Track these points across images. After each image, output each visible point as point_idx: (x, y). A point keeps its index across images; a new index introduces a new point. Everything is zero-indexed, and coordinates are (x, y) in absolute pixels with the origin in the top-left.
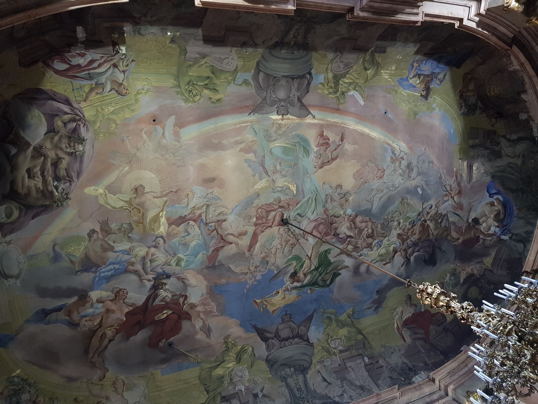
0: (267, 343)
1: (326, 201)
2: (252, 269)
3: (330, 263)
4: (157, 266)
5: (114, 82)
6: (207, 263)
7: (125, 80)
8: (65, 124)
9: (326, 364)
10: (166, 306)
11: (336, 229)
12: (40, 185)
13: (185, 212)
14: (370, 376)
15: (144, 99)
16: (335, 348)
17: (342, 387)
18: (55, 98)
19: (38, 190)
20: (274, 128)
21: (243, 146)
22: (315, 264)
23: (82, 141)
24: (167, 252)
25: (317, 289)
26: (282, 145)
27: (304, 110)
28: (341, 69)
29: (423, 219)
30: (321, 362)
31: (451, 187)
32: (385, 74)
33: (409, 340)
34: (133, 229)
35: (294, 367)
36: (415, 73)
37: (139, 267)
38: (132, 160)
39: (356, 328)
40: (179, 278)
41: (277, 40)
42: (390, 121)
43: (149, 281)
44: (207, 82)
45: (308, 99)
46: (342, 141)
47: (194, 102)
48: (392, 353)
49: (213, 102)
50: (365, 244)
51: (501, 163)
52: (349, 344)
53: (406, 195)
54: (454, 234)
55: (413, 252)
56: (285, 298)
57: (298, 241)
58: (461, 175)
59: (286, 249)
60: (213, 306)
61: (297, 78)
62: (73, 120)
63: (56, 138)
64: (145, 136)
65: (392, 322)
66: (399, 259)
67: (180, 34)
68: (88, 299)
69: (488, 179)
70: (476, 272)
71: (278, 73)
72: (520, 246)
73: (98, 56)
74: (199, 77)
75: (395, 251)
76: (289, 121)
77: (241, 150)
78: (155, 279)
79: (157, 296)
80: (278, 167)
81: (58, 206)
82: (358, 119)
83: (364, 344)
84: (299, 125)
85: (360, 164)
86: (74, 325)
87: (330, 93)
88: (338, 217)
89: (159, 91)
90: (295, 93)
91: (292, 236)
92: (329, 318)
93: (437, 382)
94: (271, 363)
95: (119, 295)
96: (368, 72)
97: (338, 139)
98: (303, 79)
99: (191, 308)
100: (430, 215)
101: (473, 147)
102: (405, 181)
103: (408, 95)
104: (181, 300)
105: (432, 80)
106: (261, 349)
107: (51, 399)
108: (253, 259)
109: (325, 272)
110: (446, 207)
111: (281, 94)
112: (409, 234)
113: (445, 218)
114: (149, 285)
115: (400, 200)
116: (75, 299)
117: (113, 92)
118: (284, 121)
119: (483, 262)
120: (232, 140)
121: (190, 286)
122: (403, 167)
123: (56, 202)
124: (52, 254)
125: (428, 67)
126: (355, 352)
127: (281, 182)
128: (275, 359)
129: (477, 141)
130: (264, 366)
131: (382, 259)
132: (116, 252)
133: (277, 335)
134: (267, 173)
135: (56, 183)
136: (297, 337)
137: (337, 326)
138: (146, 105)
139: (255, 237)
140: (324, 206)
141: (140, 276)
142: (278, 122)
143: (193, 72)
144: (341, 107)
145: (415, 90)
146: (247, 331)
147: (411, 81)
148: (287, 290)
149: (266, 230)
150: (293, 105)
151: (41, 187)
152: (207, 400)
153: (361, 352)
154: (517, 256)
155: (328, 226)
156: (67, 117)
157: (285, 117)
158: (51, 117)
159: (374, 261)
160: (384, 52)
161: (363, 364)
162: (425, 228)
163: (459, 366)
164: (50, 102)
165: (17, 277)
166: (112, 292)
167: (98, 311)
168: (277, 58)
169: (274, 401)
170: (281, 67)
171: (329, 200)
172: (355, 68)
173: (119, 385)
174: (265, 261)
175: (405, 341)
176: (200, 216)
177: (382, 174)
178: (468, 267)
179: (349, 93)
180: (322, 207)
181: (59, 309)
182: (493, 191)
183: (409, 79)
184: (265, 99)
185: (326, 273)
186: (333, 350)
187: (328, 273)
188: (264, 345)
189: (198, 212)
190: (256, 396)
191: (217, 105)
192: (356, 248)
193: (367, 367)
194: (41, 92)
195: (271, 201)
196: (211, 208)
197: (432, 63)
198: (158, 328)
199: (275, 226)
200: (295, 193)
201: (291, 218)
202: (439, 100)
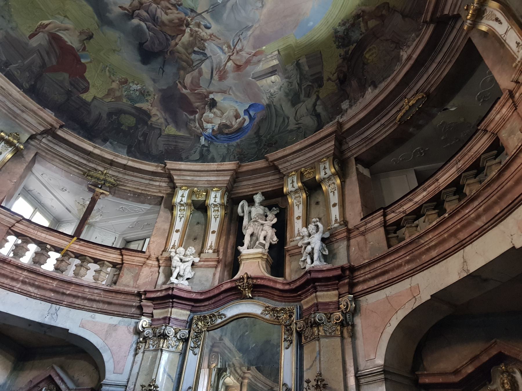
29: (189, 19)
31: (241, 50)
51: (288, 110)
55: (144, 20)
58: (259, 61)
69: (265, 101)
70: (154, 119)
72: (197, 156)
100: (197, 29)
101: (298, 65)
110: (216, 53)
119: (168, 125)
129: (307, 68)
154: (184, 156)
163: (18, 101)
178: (158, 110)
182: (252, 113)
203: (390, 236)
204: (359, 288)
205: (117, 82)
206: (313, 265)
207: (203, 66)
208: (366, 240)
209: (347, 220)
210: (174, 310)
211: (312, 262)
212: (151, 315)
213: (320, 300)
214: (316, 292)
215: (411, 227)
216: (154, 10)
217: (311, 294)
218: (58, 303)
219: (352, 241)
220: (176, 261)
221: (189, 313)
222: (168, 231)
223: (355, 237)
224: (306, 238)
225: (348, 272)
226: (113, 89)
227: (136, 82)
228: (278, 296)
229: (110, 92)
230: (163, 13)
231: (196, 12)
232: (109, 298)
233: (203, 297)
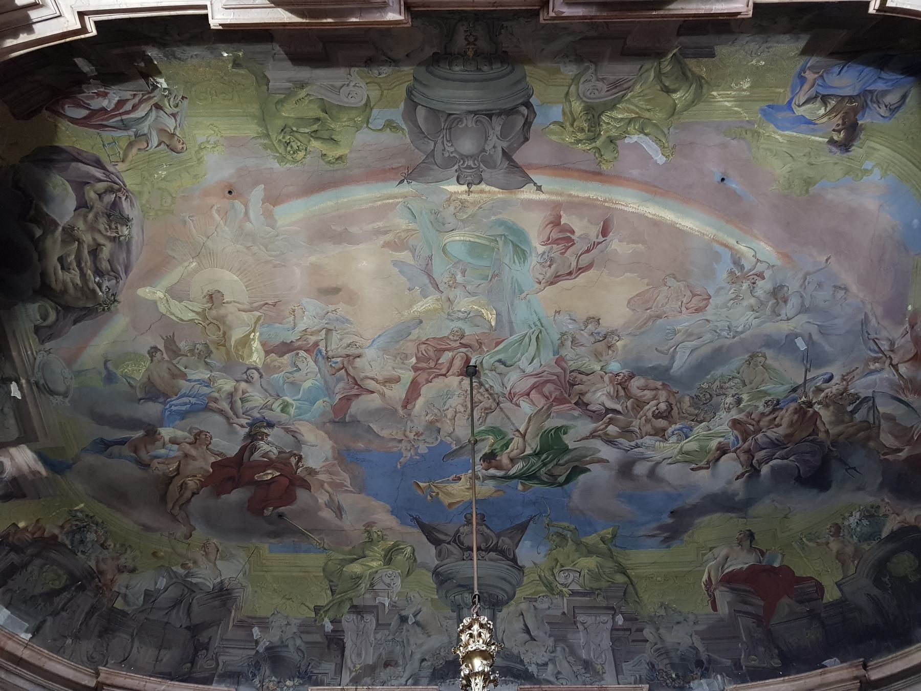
0: (439, 547)
1: (562, 344)
2: (411, 436)
3: (566, 450)
4: (252, 409)
5: (162, 131)
6: (332, 416)
7: (178, 129)
8: (100, 195)
9: (539, 605)
10: (270, 464)
11: (582, 394)
12: (78, 281)
13: (292, 337)
14: (613, 650)
15: (212, 158)
17: (552, 652)
18: (80, 158)
19: (75, 286)
20: (452, 208)
21: (389, 237)
23: (126, 221)
24: (266, 390)
25: (536, 487)
26: (468, 239)
27: (517, 174)
28: (603, 93)
29: (803, 399)
30: (530, 600)
31: (892, 344)
33: (724, 609)
34: (211, 352)
36: (812, 92)
37: (225, 406)
38: (200, 252)
39: (617, 562)
40: (287, 430)
41: (435, 50)
42: (734, 197)
43: (242, 426)
44: (315, 127)
45: (524, 155)
47: (295, 161)
48: (678, 623)
49: (329, 162)
50: (648, 428)
52: (595, 585)
53: (764, 350)
54: (887, 439)
57: (498, 404)
60: (345, 478)
61: (499, 114)
62: (110, 190)
63: (91, 216)
64: (216, 216)
65: (702, 568)
66: (730, 466)
67: (244, 54)
68: (158, 437)
71: (454, 107)
73: (128, 95)
74: (302, 119)
75: (723, 450)
76: (484, 195)
77: (386, 245)
78: (251, 425)
79: (254, 449)
80: (459, 277)
81: (104, 310)
83: (625, 593)
84: (505, 203)
85: (646, 281)
86: (144, 465)
87: (579, 141)
88: (588, 375)
89: (234, 144)
90: (495, 144)
91: (487, 395)
92: (563, 537)
94: (441, 578)
95: (199, 438)
96: (674, 96)
97: (594, 232)
99: (310, 474)
100: (823, 395)
102: (764, 322)
103: (791, 141)
104: (293, 461)
105: (864, 107)
106: (428, 554)
107: (122, 545)
108: (412, 421)
109: (555, 462)
110: (874, 382)
111: (467, 145)
112: (761, 423)
113: (865, 406)
114: (243, 432)
115: (746, 357)
116: (140, 434)
117: (162, 146)
120: (370, 227)
121: (305, 443)
122: (759, 292)
123: (101, 305)
124: (104, 373)
125: (847, 80)
126: (601, 601)
127: (464, 304)
130: (429, 579)
131: (687, 458)
132: (189, 381)
133: (457, 539)
134: (436, 286)
135: (97, 279)
137: (576, 550)
138: (217, 167)
139: (414, 390)
140: (556, 352)
141: (228, 418)
142: (460, 197)
143: (289, 112)
144: (604, 167)
146: (403, 523)
149: (436, 380)
151: (79, 282)
152: (330, 602)
153: (614, 604)
155: (566, 388)
156: (101, 186)
157: (474, 188)
158: (80, 185)
159: (669, 461)
160: (712, 55)
161: (609, 625)
162: (805, 415)
164: (74, 164)
165: (65, 395)
166: (190, 432)
167: (173, 454)
168: (448, 79)
169: (429, 636)
170: (459, 93)
172: (638, 88)
173: (212, 550)
174: (433, 427)
175: (715, 608)
176: (316, 344)
177: (702, 304)
179: (627, 141)
180: (551, 353)
181: (122, 442)
183: (793, 106)
184: (432, 154)
188: (432, 550)
189: (313, 339)
190: (404, 619)
191: (336, 166)
193: (614, 632)
194: (59, 150)
195: (446, 333)
196: (335, 336)
198: (259, 490)
199: (453, 375)
200: (493, 324)
201: (485, 365)
202: (883, 152)
205: (832, 539)
207: (881, 409)
216: (765, 439)
226: (837, 552)
229: (840, 556)
230: (775, 430)
231: (798, 387)
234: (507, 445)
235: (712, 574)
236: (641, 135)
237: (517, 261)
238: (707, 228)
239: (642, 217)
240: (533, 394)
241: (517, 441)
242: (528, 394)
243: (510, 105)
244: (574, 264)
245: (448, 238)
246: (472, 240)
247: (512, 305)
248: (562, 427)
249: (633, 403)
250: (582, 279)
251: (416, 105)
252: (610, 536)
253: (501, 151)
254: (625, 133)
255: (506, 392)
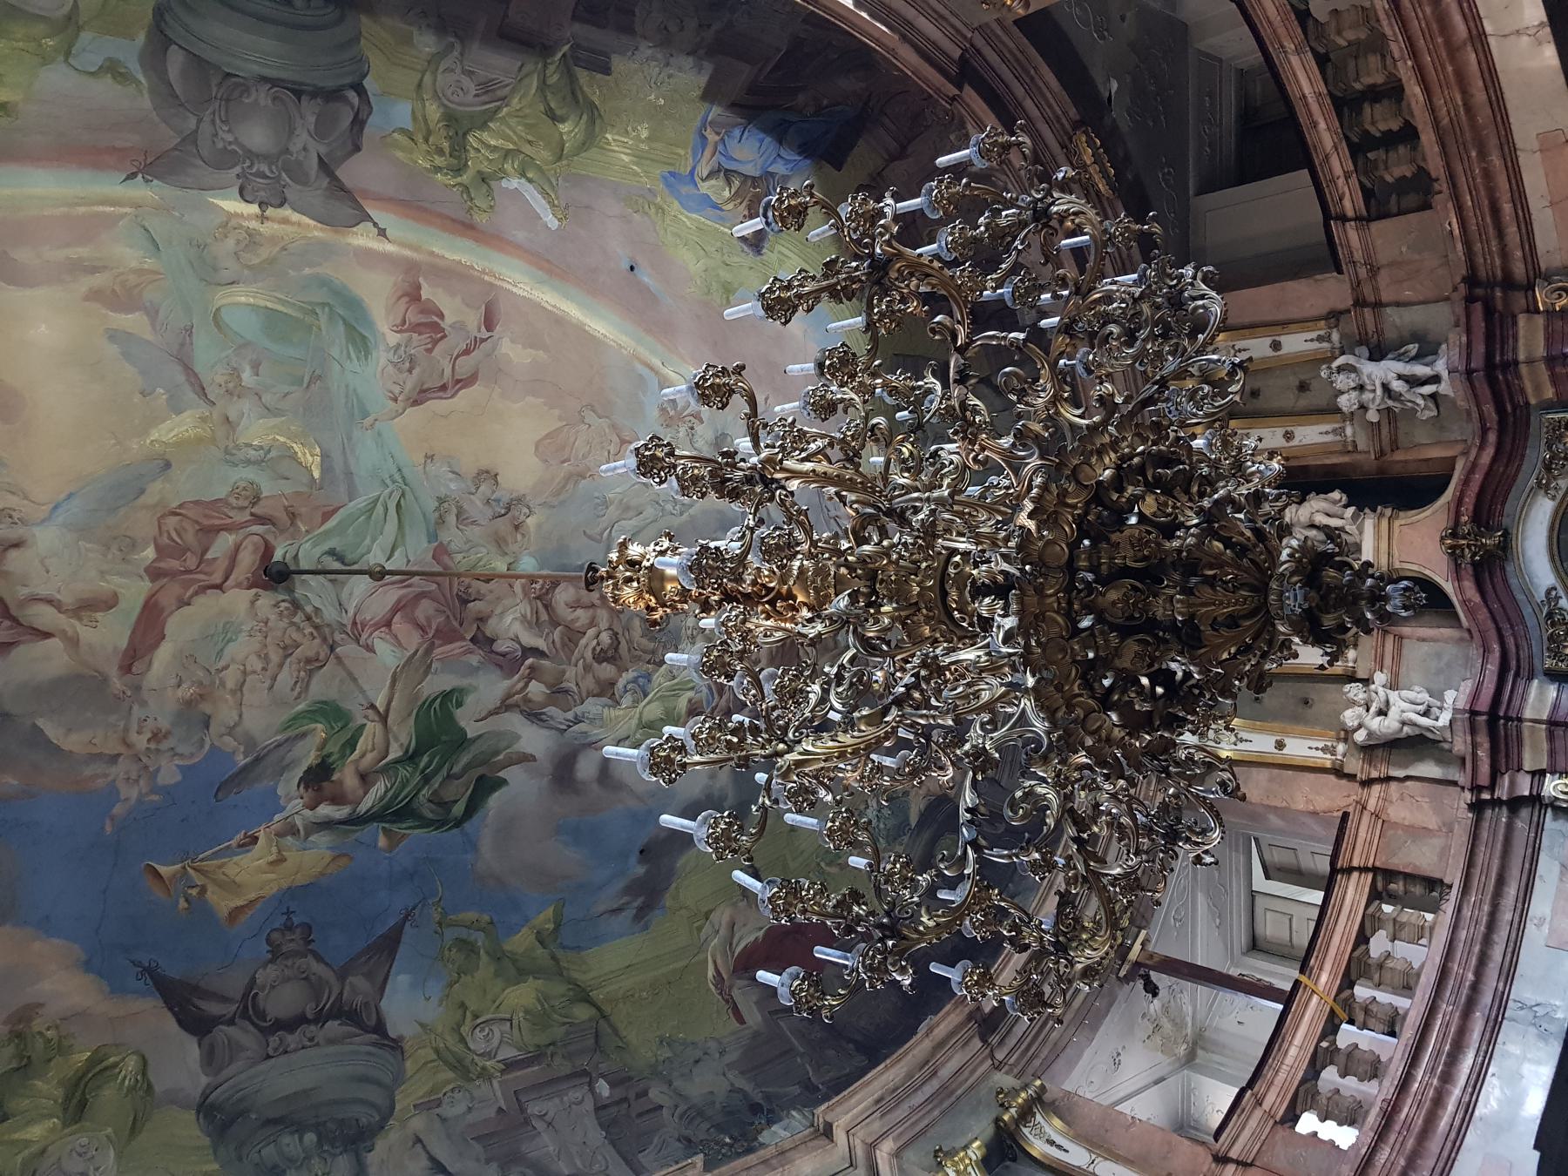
0: (207, 1040)
1: (441, 521)
2: (141, 742)
3: (461, 741)
9: (448, 1111)
11: (482, 620)
14: (613, 1143)
16: (487, 1055)
20: (230, 243)
21: (98, 280)
22: (404, 739)
26: (262, 303)
27: (346, 205)
28: (470, 98)
30: (429, 1105)
32: (621, 149)
35: (318, 1128)
39: (571, 981)
45: (357, 172)
46: (489, 327)
48: (697, 1062)
50: (589, 683)
52: (543, 1039)
56: (281, 860)
57: (332, 649)
59: (286, 677)
61: (314, 94)
65: (701, 957)
76: (289, 228)
77: (95, 295)
80: (247, 376)
82: (541, 269)
83: (597, 1036)
85: (556, 412)
87: (438, 169)
88: (488, 581)
90: (306, 145)
91: (308, 630)
93: (840, 1135)
94: (220, 1118)
96: (564, 128)
97: (473, 320)
98: (340, 102)
106: (181, 1064)
108: (143, 704)
109: (444, 770)
111: (257, 136)
118: (268, 224)
126: (562, 1067)
127: (257, 431)
128: (241, 1100)
130: (188, 1129)
133: (249, 1009)
134: (202, 391)
136: (335, 1018)
137: (497, 974)
140: (433, 536)
142: (246, 224)
144: (480, 219)
145: (722, 218)
146: (117, 989)
147: (705, 188)
148: (293, 831)
149: (201, 600)
150: (300, 177)
153: (583, 1062)
157: (270, 211)
160: (606, 70)
161: (589, 1105)
163: (909, 1076)
171: (451, 519)
174: (194, 715)
175: (741, 1020)
179: (504, 183)
180: (424, 539)
184: (192, 139)
185: (449, 776)
186: (481, 1062)
187: (458, 777)
188: (192, 1049)
192: (558, 693)
195: (221, 492)
197: (761, 141)
199: (238, 585)
200: (316, 474)
203: (1394, 210)
204: (1519, 270)
206: (1445, 374)
208: (1391, 264)
209: (1324, 311)
210: (1528, 713)
211: (1435, 379)
212: (1539, 774)
213: (1541, 351)
214: (1516, 363)
215: (1386, 162)
217: (1519, 377)
218: (1501, 1002)
219: (1386, 296)
220: (1386, 726)
221: (1535, 682)
222: (1276, 771)
223: (1376, 289)
224: (1367, 396)
225: (1479, 292)
227: (862, 807)
228: (1507, 466)
232: (1484, 881)
233: (1496, 647)
234: (351, 744)
235: (719, 962)
236: (523, 180)
237: (353, 355)
238: (624, 338)
239: (538, 307)
240: (398, 624)
241: (373, 729)
242: (388, 624)
243: (330, 84)
244: (448, 371)
245: (223, 297)
246: (269, 305)
247: (349, 439)
248: (452, 691)
249: (562, 634)
250: (464, 398)
251: (167, 42)
252: (551, 926)
253: (316, 160)
254: (501, 174)
255: (347, 620)
